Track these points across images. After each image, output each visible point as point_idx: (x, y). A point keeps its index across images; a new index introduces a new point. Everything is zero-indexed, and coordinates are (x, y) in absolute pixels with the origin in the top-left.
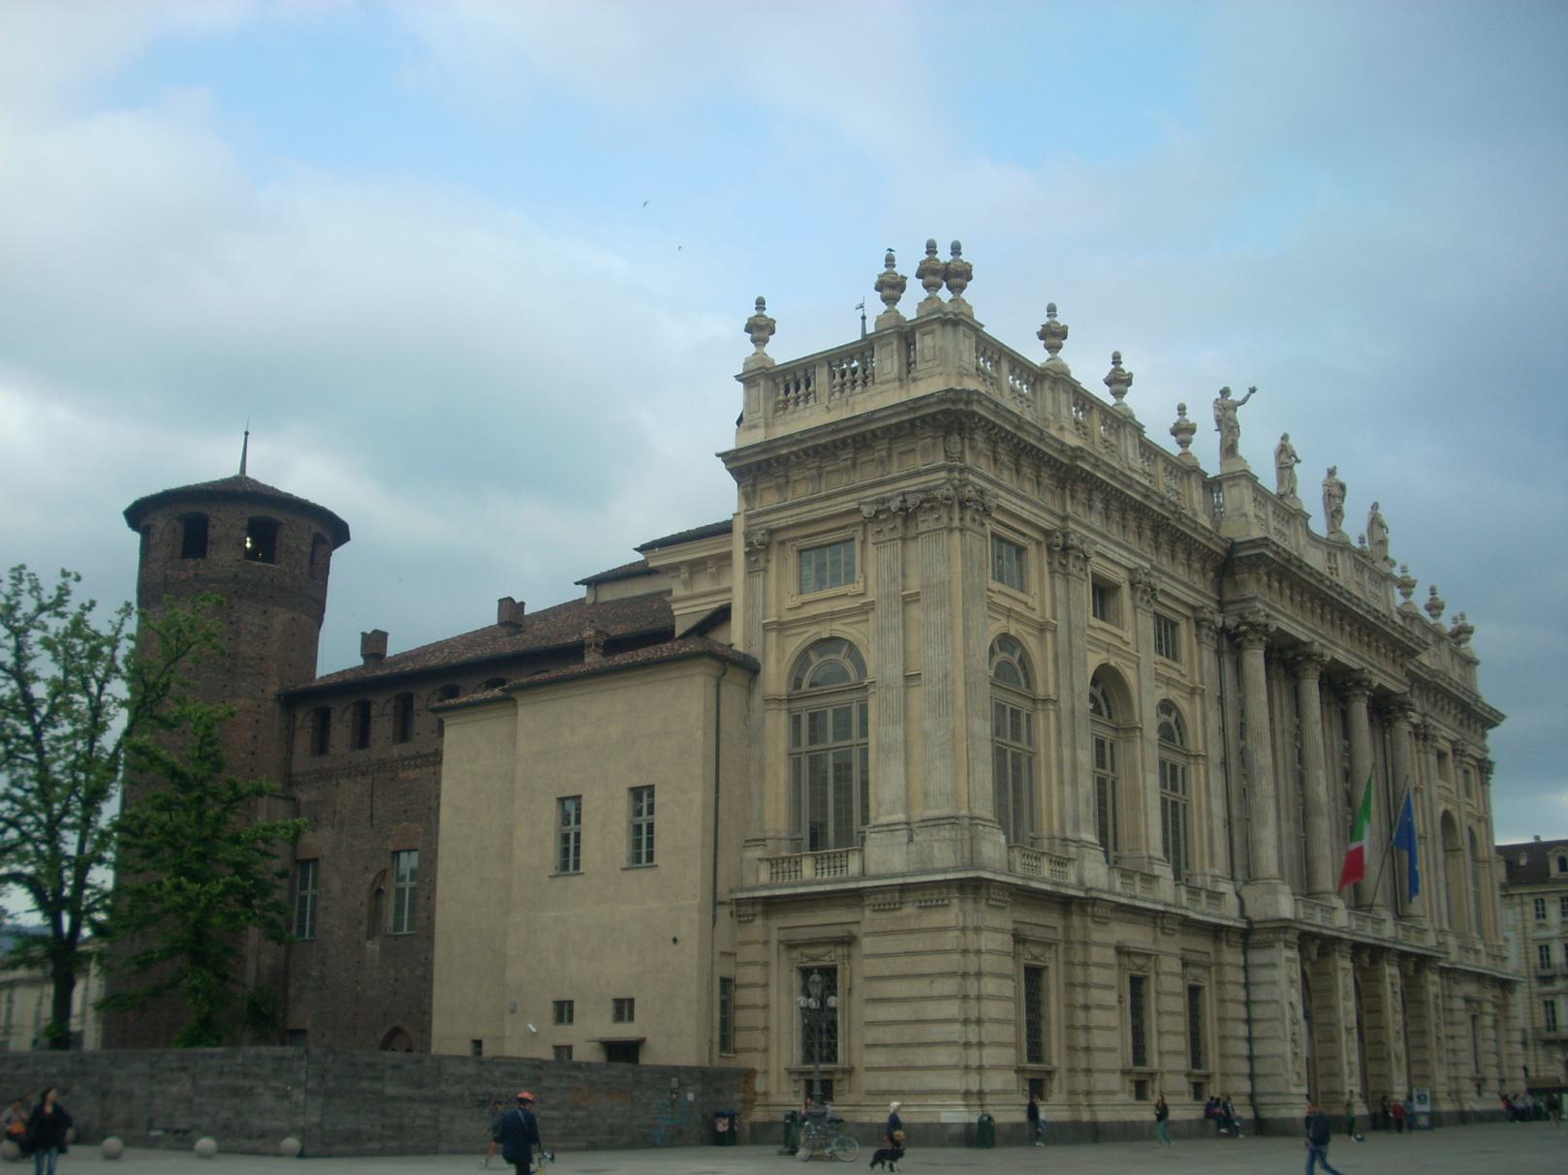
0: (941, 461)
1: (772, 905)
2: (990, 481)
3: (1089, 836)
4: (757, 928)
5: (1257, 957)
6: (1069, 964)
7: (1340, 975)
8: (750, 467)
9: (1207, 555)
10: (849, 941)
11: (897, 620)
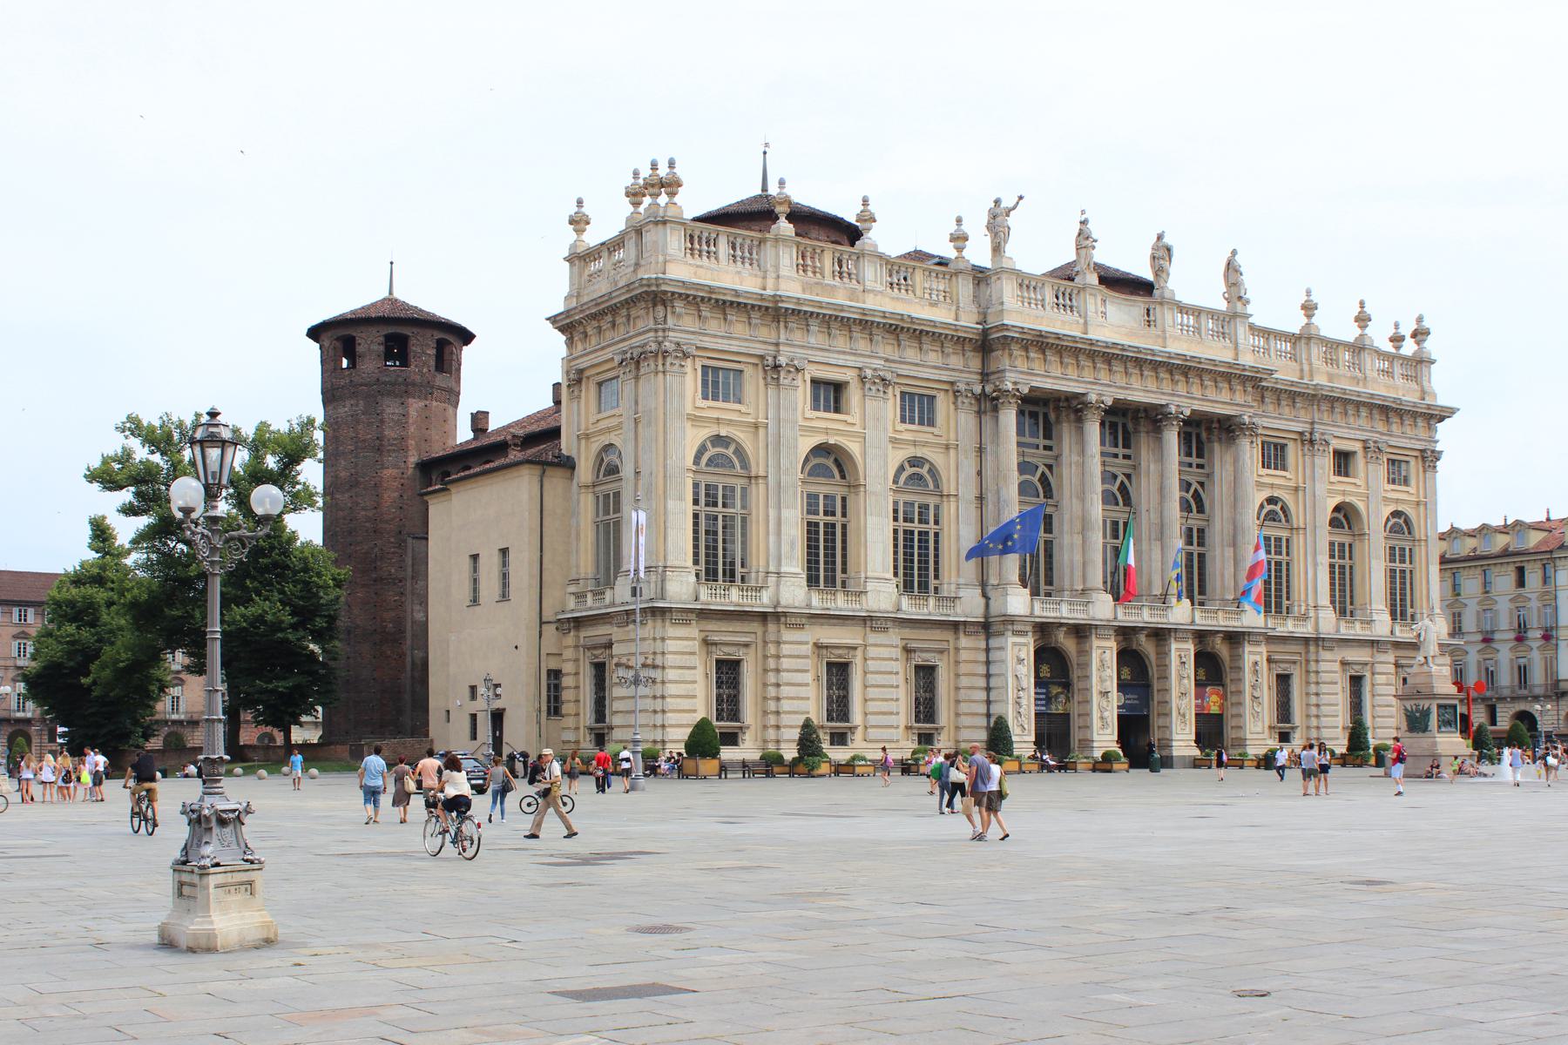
0: (652, 325)
1: (578, 623)
2: (693, 333)
3: (795, 565)
4: (570, 639)
5: (994, 643)
6: (765, 657)
7: (1095, 655)
8: (567, 324)
9: (960, 342)
10: (609, 645)
11: (632, 435)
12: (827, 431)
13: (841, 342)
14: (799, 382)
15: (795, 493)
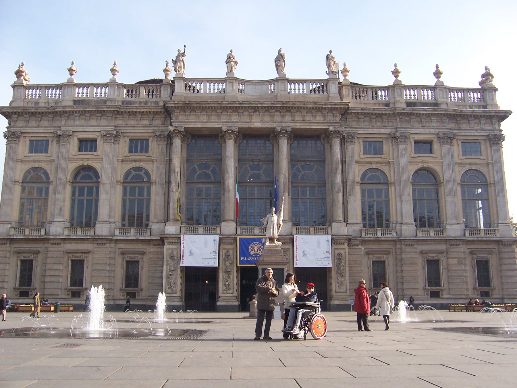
9: (156, 113)
12: (82, 160)
13: (93, 122)
14: (71, 142)
15: (65, 187)
